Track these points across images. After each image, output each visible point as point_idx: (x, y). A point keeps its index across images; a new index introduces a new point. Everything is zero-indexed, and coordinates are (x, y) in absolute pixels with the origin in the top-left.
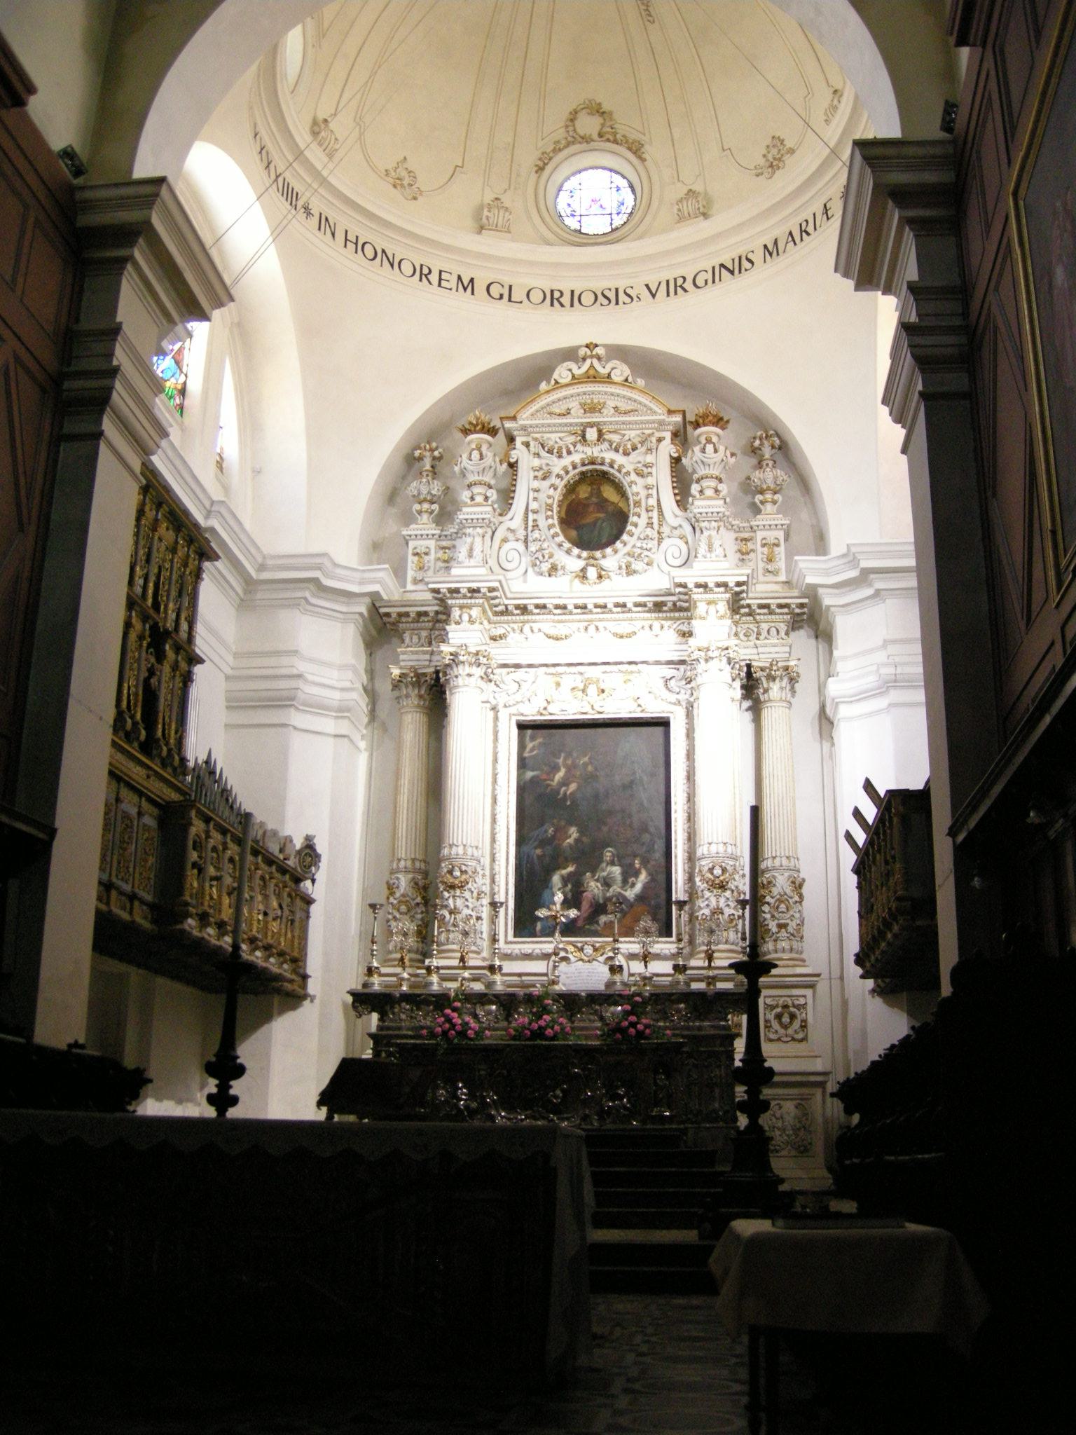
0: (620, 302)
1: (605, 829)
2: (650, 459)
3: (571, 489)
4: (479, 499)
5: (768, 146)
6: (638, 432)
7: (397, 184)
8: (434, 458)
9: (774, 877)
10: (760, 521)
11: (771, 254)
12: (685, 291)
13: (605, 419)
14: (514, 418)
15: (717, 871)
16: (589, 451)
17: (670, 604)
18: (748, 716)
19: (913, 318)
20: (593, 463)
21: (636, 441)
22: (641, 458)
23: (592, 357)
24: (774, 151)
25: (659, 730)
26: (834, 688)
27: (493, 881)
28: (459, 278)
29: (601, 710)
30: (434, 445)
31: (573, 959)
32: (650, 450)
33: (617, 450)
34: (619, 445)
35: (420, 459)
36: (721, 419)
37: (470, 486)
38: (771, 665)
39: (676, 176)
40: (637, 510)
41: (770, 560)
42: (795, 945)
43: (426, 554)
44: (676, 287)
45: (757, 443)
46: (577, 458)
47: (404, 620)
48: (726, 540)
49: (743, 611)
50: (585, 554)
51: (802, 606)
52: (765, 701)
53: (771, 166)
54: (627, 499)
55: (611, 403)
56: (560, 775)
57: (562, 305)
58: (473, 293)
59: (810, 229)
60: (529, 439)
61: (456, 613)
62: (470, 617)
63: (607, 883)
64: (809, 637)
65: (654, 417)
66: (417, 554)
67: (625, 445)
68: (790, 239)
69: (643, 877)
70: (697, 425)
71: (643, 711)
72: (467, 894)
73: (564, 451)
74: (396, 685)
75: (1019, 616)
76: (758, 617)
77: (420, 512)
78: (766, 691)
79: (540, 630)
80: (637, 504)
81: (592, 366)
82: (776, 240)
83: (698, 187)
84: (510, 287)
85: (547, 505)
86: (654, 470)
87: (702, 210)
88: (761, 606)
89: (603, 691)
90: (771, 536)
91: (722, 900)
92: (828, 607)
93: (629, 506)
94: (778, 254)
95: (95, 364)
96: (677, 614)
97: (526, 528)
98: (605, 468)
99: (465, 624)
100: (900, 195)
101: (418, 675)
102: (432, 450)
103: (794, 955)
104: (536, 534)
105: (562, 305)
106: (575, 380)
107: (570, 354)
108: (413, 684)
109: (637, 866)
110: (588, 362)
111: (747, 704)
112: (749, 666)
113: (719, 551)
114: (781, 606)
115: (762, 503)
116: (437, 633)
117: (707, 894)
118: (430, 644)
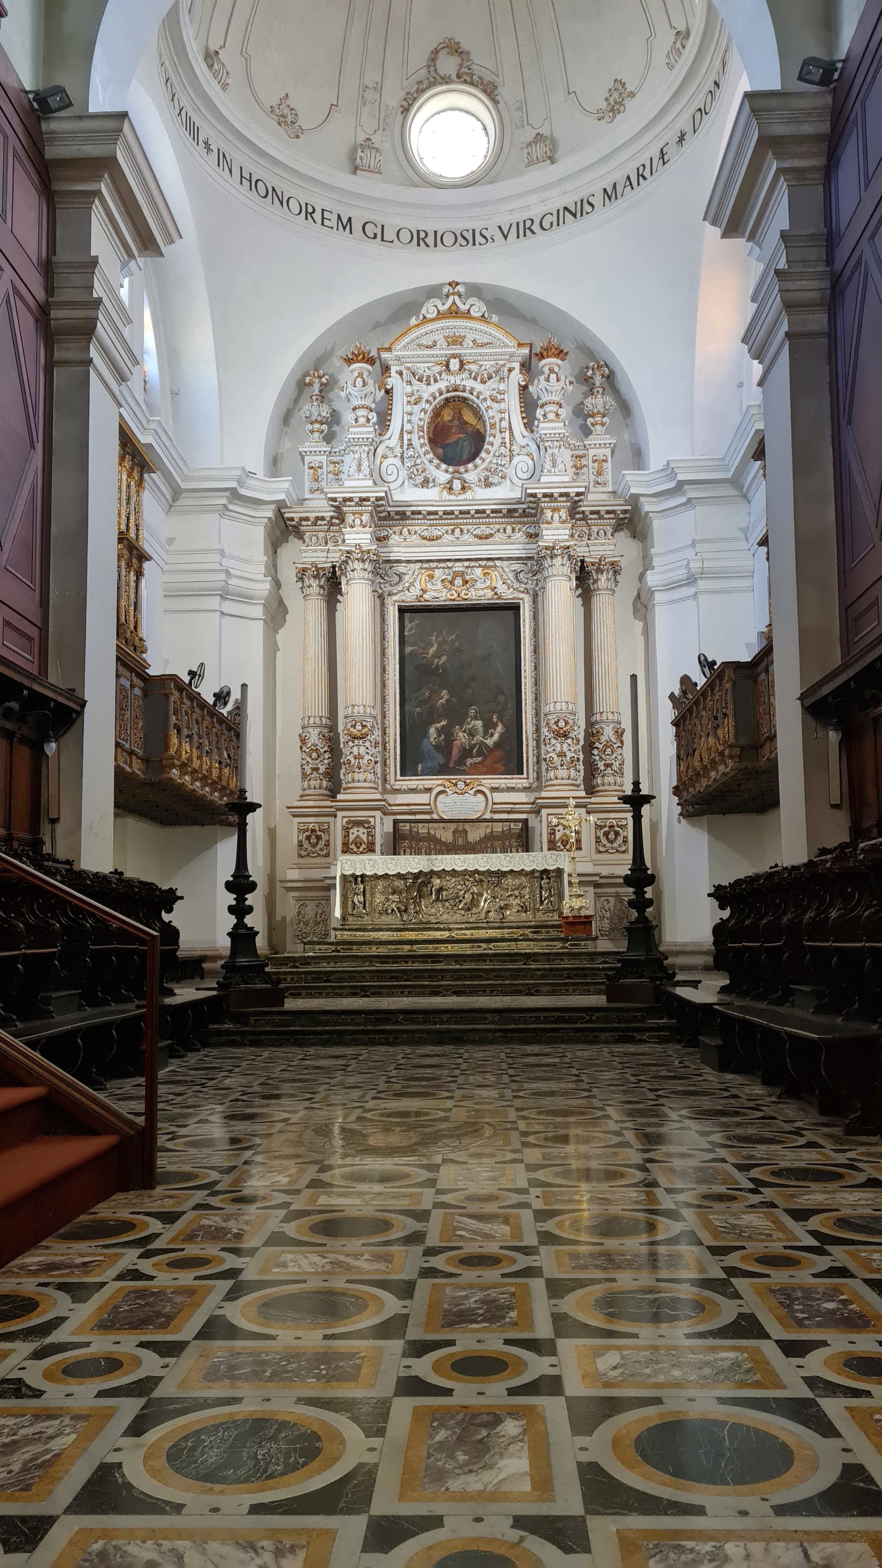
0: (477, 243)
1: (469, 691)
2: (502, 387)
3: (437, 413)
4: (362, 420)
5: (610, 90)
6: (492, 363)
7: (282, 121)
8: (322, 384)
9: (602, 728)
11: (610, 198)
12: (533, 233)
13: (466, 351)
14: (389, 349)
15: (562, 724)
16: (452, 379)
17: (520, 511)
18: (580, 601)
19: (782, 264)
20: (456, 390)
21: (491, 370)
22: (495, 386)
23: (454, 294)
24: (616, 95)
25: (511, 612)
26: (652, 579)
27: (384, 733)
28: (339, 217)
29: (466, 597)
30: (321, 372)
31: (450, 792)
32: (502, 379)
33: (475, 379)
34: (477, 374)
35: (310, 384)
36: (562, 351)
37: (354, 409)
38: (600, 560)
39: (525, 119)
40: (493, 431)
41: (599, 473)
42: (618, 780)
43: (320, 467)
44: (525, 229)
45: (590, 373)
46: (442, 385)
47: (304, 523)
48: (565, 457)
49: (578, 516)
50: (451, 469)
51: (625, 512)
52: (595, 590)
53: (612, 110)
54: (484, 422)
55: (470, 337)
57: (427, 246)
58: (351, 233)
59: (647, 173)
60: (402, 368)
61: (349, 518)
62: (362, 521)
63: (472, 733)
64: (626, 537)
65: (507, 350)
66: (312, 468)
67: (483, 375)
68: (628, 183)
69: (500, 728)
70: (541, 357)
71: (499, 598)
72: (368, 744)
73: (432, 380)
75: (873, 527)
76: (589, 521)
77: (312, 432)
78: (595, 581)
79: (416, 532)
80: (493, 426)
81: (454, 303)
82: (615, 184)
83: (545, 131)
84: (383, 226)
85: (419, 426)
86: (506, 397)
87: (549, 154)
88: (592, 513)
89: (467, 582)
90: (601, 453)
91: (565, 746)
92: (647, 513)
93: (485, 426)
94: (616, 198)
95: (78, 296)
96: (525, 519)
97: (402, 447)
98: (466, 395)
99: (358, 528)
101: (317, 569)
102: (320, 377)
103: (617, 788)
104: (411, 453)
105: (427, 246)
106: (441, 316)
107: (433, 292)
108: (315, 577)
109: (495, 720)
110: (451, 298)
111: (580, 591)
112: (582, 561)
113: (561, 466)
114: (608, 512)
115: (593, 425)
116: (332, 534)
117: (553, 741)
118: (326, 543)
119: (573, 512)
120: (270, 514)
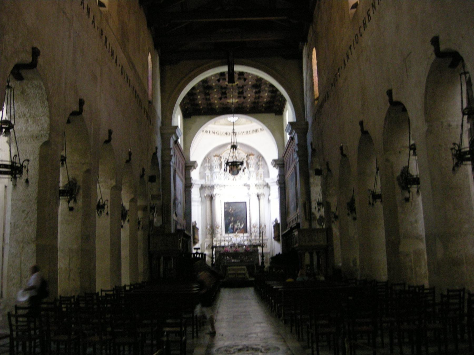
10: (259, 170)
44: (246, 133)
48: (254, 175)
56: (230, 210)
74: (206, 197)
100: (278, 165)
119: (256, 185)
120: (200, 186)
